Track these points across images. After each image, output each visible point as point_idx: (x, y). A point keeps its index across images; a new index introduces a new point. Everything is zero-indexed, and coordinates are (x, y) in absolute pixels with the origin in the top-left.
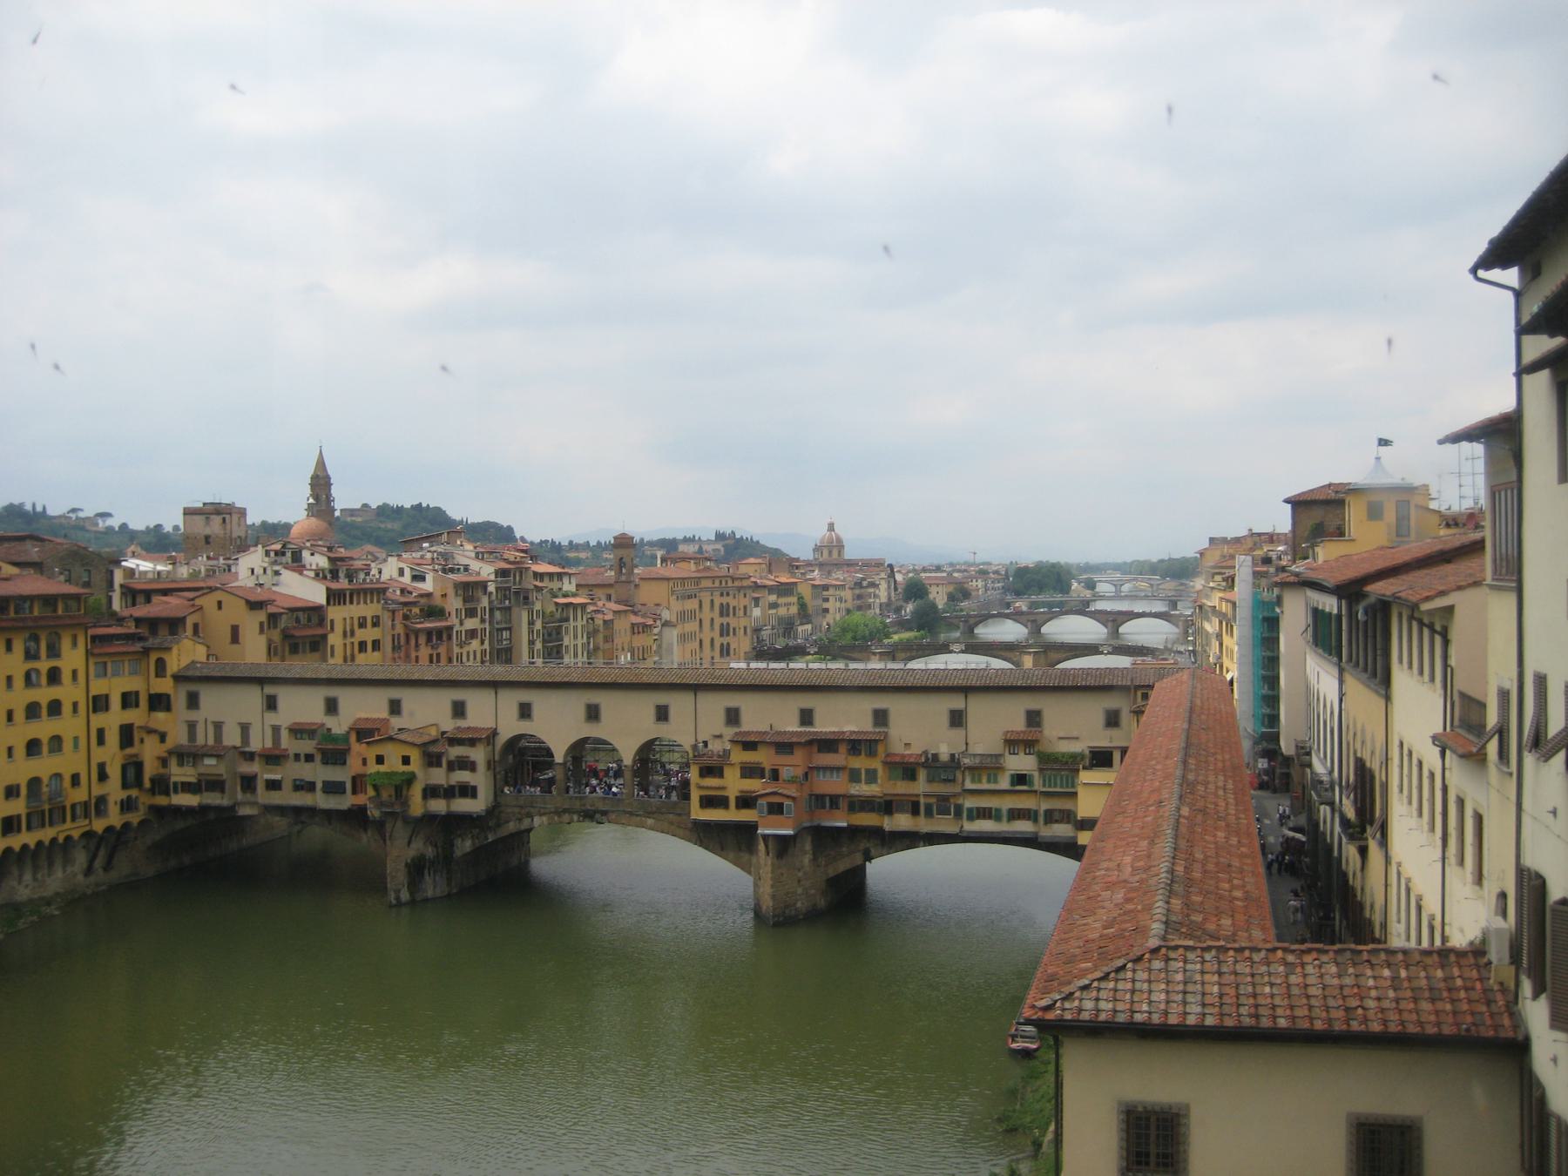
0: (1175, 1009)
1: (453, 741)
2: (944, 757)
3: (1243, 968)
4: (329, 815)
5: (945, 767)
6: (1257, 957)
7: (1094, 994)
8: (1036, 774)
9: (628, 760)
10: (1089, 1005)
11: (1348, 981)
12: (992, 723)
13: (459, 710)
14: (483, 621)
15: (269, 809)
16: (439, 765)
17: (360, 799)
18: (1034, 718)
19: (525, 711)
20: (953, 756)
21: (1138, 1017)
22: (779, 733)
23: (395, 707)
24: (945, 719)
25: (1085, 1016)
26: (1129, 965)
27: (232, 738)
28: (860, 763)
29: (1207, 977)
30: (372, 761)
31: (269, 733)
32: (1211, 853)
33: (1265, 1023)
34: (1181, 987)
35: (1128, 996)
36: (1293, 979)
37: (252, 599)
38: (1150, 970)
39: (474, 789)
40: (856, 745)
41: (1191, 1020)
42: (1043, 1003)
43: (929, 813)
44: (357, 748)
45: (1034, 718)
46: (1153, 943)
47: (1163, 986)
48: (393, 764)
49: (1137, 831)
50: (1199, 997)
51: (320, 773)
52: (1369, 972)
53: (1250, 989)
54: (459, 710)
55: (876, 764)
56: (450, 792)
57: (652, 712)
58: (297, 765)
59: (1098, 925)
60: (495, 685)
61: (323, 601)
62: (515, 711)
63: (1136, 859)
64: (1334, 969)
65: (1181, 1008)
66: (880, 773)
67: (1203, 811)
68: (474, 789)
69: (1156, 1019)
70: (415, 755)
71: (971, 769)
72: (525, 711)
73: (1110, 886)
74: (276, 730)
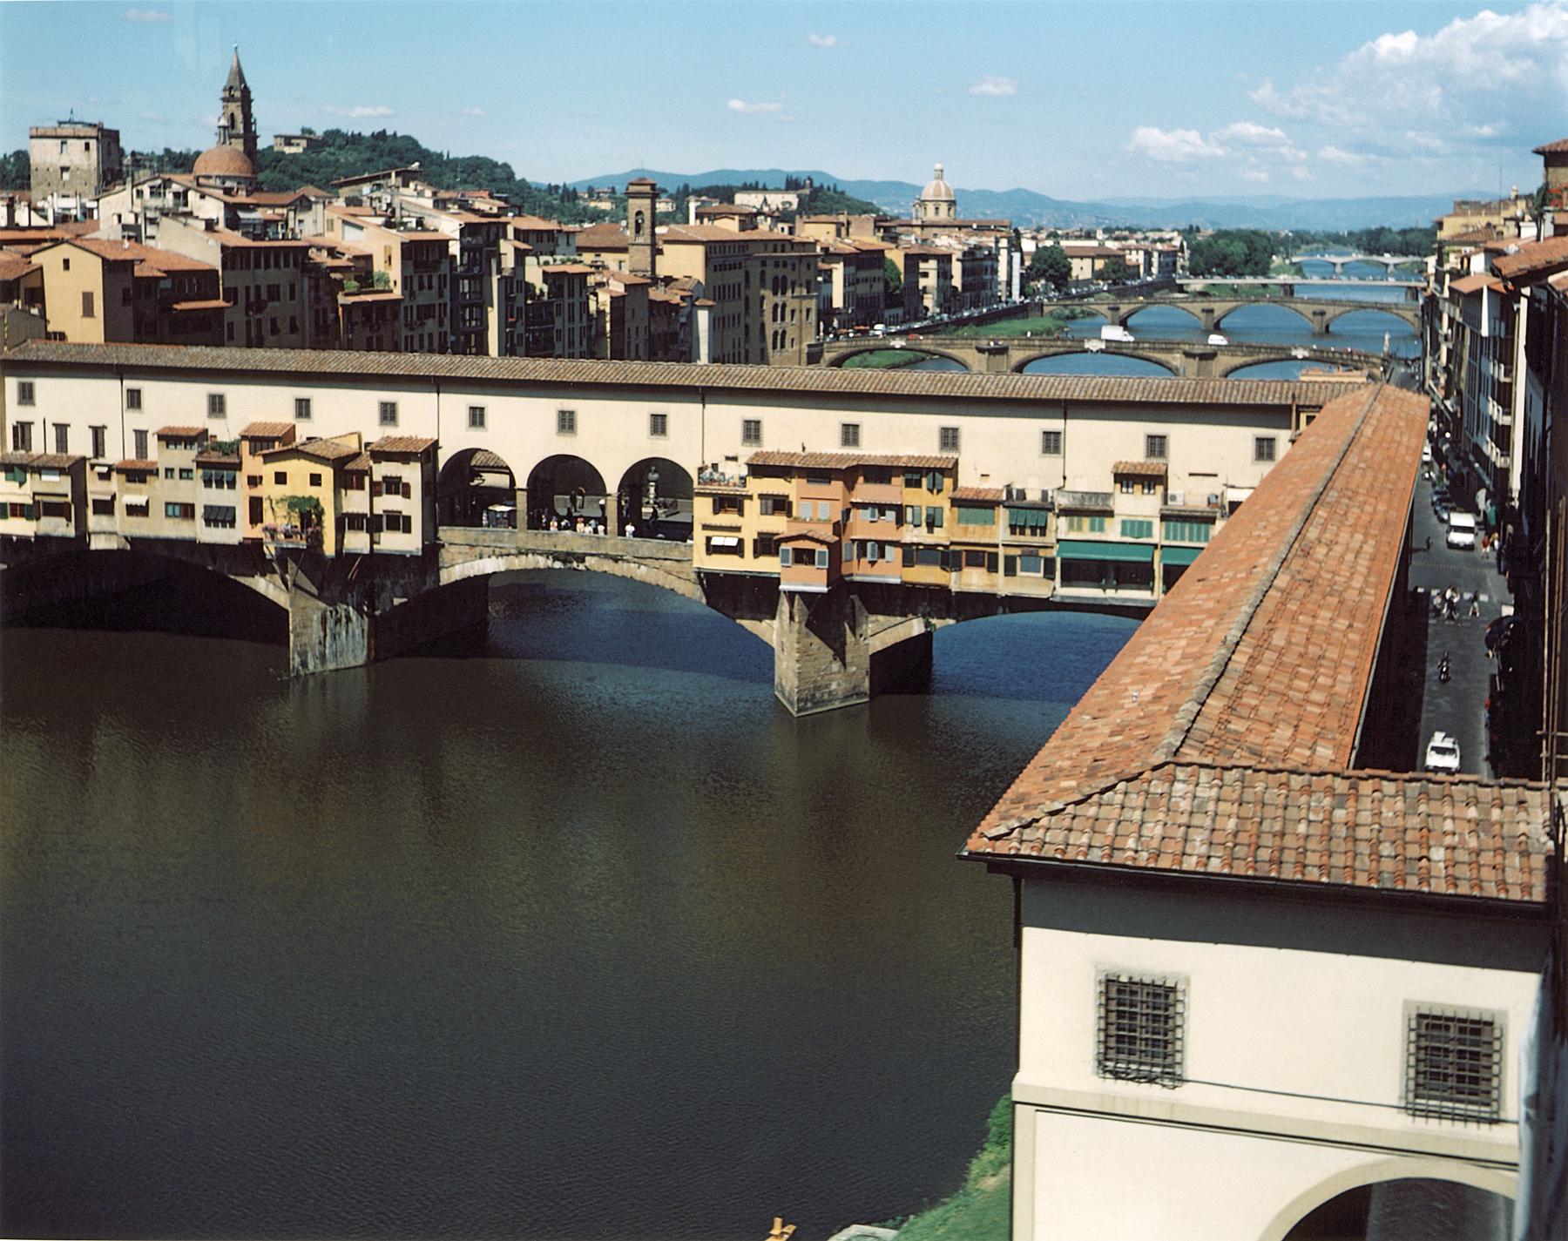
0: (1173, 847)
1: (380, 456)
2: (1033, 496)
3: (1275, 796)
4: (213, 548)
5: (1033, 507)
6: (1296, 782)
7: (1067, 823)
8: (1157, 522)
9: (612, 486)
10: (1056, 836)
11: (1414, 821)
12: (1098, 449)
13: (389, 413)
14: (441, 295)
15: (133, 541)
16: (362, 488)
17: (257, 532)
18: (1157, 445)
19: (477, 417)
20: (1045, 493)
21: (1119, 858)
22: (811, 455)
23: (303, 408)
24: (1037, 442)
25: (1049, 851)
26: (1121, 786)
27: (80, 445)
28: (920, 498)
29: (1223, 806)
30: (269, 479)
31: (131, 440)
32: (1298, 639)
33: (1289, 873)
34: (1184, 819)
35: (1110, 829)
36: (1340, 814)
37: (111, 257)
38: (1147, 793)
39: (408, 519)
40: (914, 474)
41: (1190, 864)
42: (994, 832)
43: (1010, 570)
44: (252, 464)
45: (1157, 445)
46: (1158, 758)
47: (1161, 816)
48: (297, 486)
49: (1211, 604)
50: (1207, 833)
51: (204, 496)
52: (1448, 811)
53: (1278, 827)
54: (389, 413)
55: (942, 501)
56: (373, 524)
57: (645, 424)
58: (169, 481)
59: (1107, 731)
60: (439, 384)
61: (214, 260)
62: (464, 416)
63: (1192, 641)
64: (1400, 805)
65: (1178, 849)
66: (947, 513)
67: (1310, 582)
68: (408, 519)
69: (1143, 859)
70: (327, 473)
71: (1066, 512)
72: (477, 417)
73: (1144, 676)
74: (141, 435)
